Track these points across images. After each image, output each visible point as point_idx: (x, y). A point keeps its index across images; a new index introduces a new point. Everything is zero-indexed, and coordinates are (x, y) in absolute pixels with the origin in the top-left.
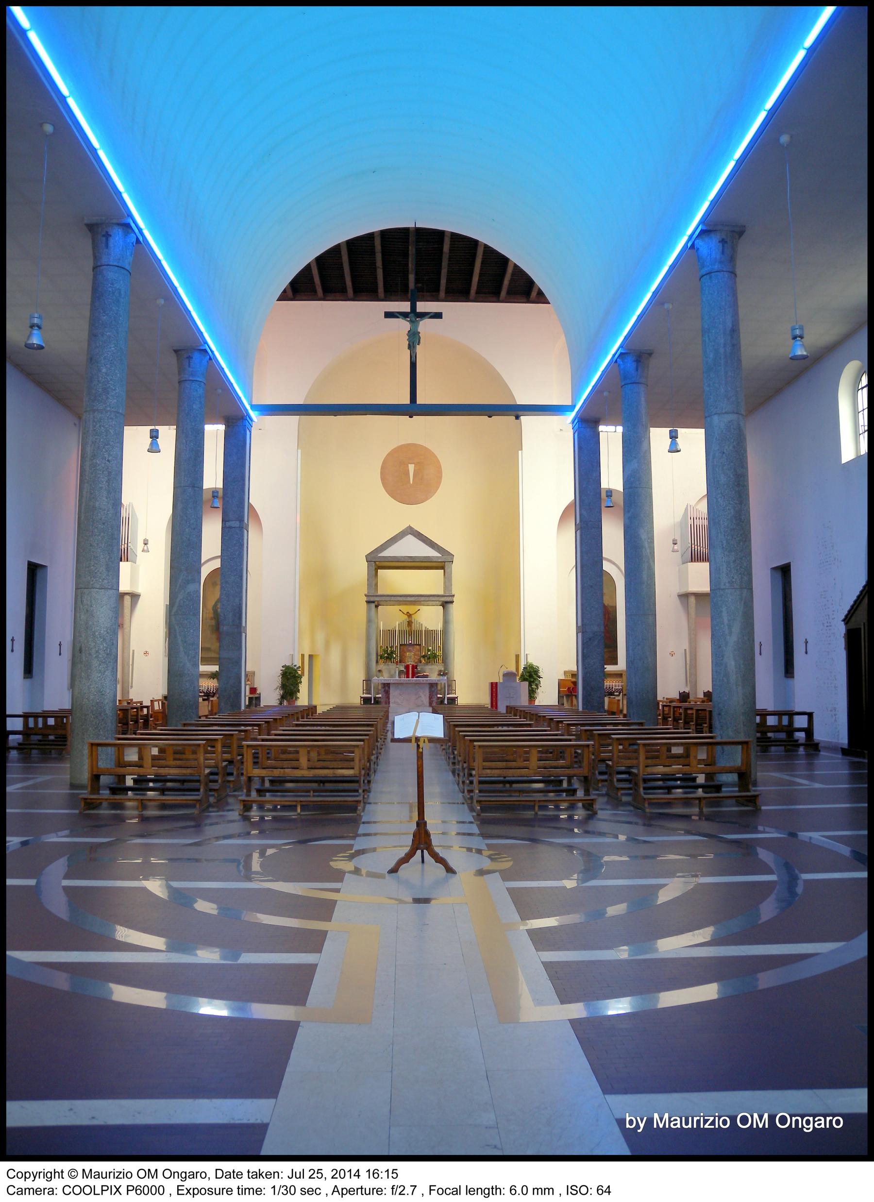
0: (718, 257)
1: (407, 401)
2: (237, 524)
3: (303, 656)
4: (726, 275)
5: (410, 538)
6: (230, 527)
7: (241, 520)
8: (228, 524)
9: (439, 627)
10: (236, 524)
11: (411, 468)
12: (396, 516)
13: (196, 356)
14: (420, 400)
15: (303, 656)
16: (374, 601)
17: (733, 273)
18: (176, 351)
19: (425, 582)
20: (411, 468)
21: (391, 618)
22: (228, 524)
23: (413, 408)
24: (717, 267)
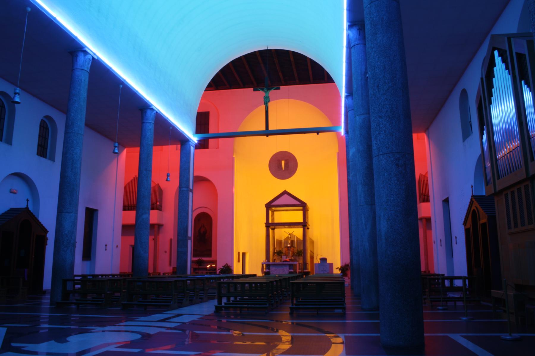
0: (357, 37)
1: (263, 128)
2: (185, 189)
3: (239, 253)
4: (362, 45)
5: (286, 195)
6: (183, 191)
7: (188, 187)
8: (182, 189)
9: (301, 237)
10: (185, 189)
11: (283, 162)
12: (278, 186)
13: (149, 112)
14: (270, 128)
15: (239, 253)
16: (270, 226)
17: (365, 44)
18: (141, 110)
19: (297, 216)
20: (283, 162)
21: (282, 234)
22: (182, 189)
23: (268, 133)
24: (357, 43)
